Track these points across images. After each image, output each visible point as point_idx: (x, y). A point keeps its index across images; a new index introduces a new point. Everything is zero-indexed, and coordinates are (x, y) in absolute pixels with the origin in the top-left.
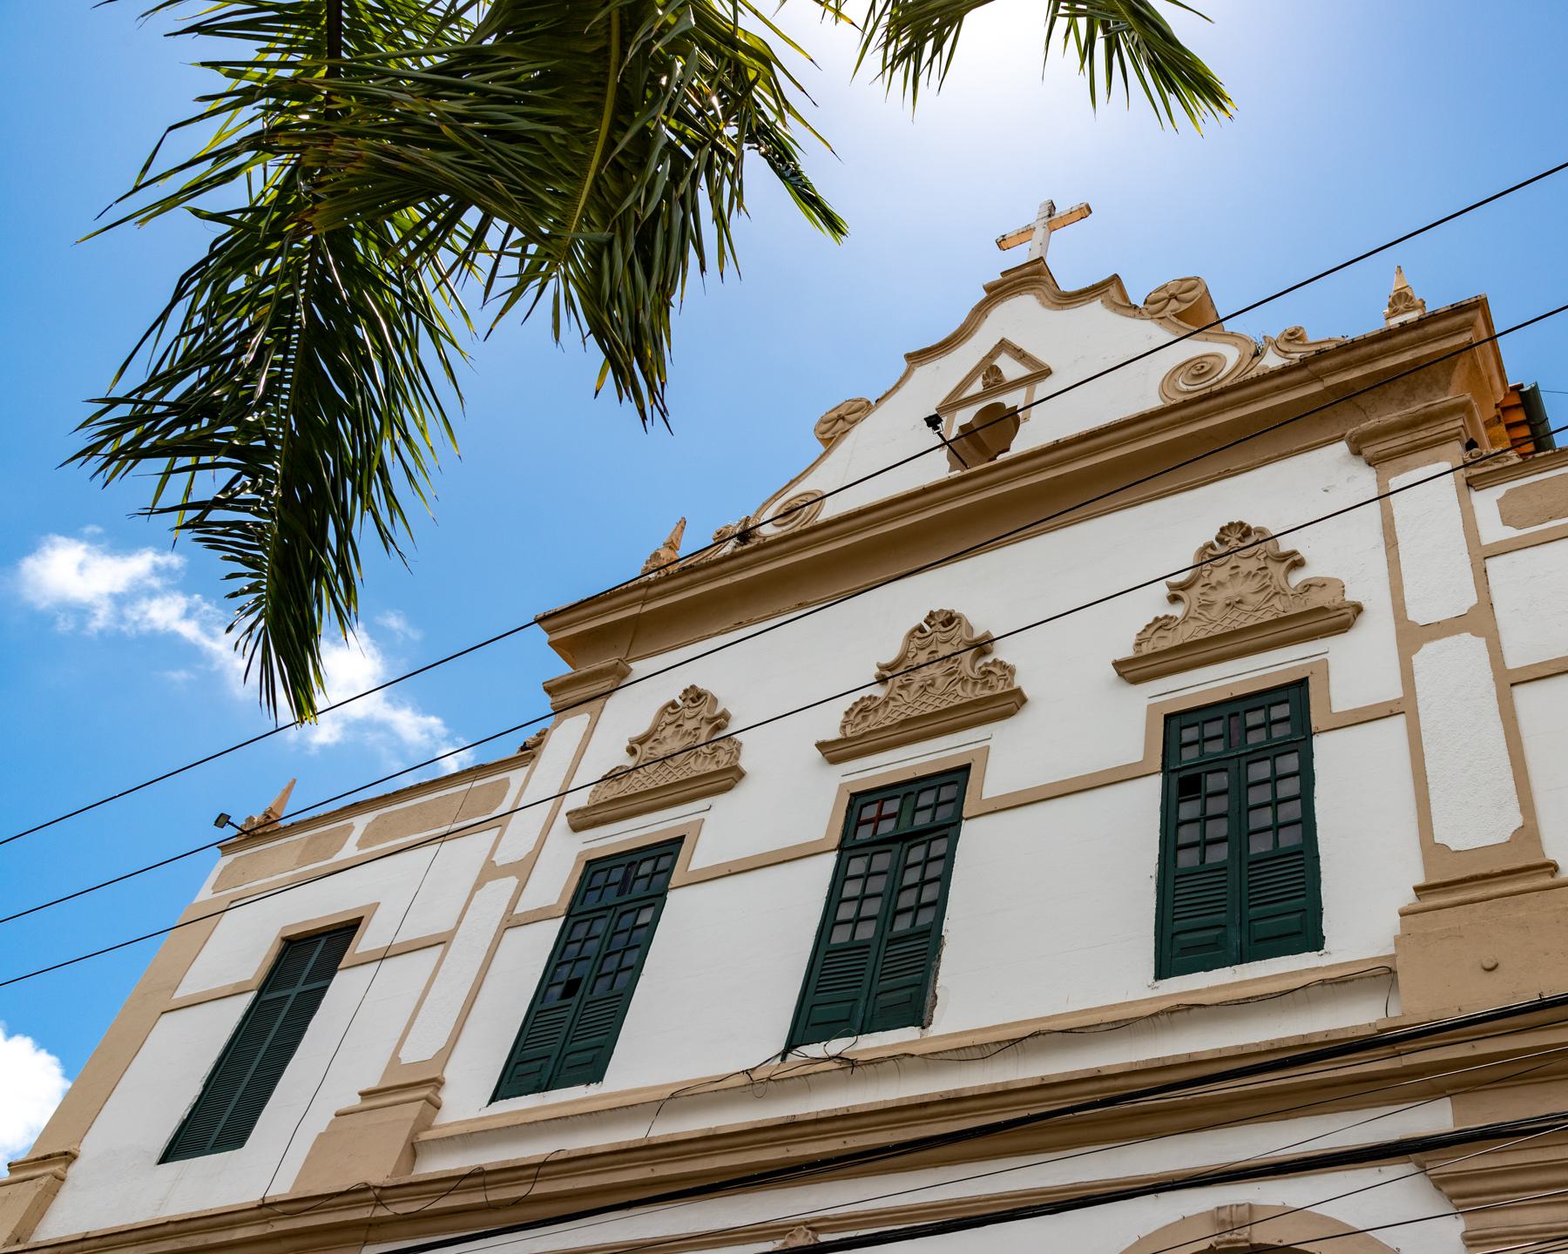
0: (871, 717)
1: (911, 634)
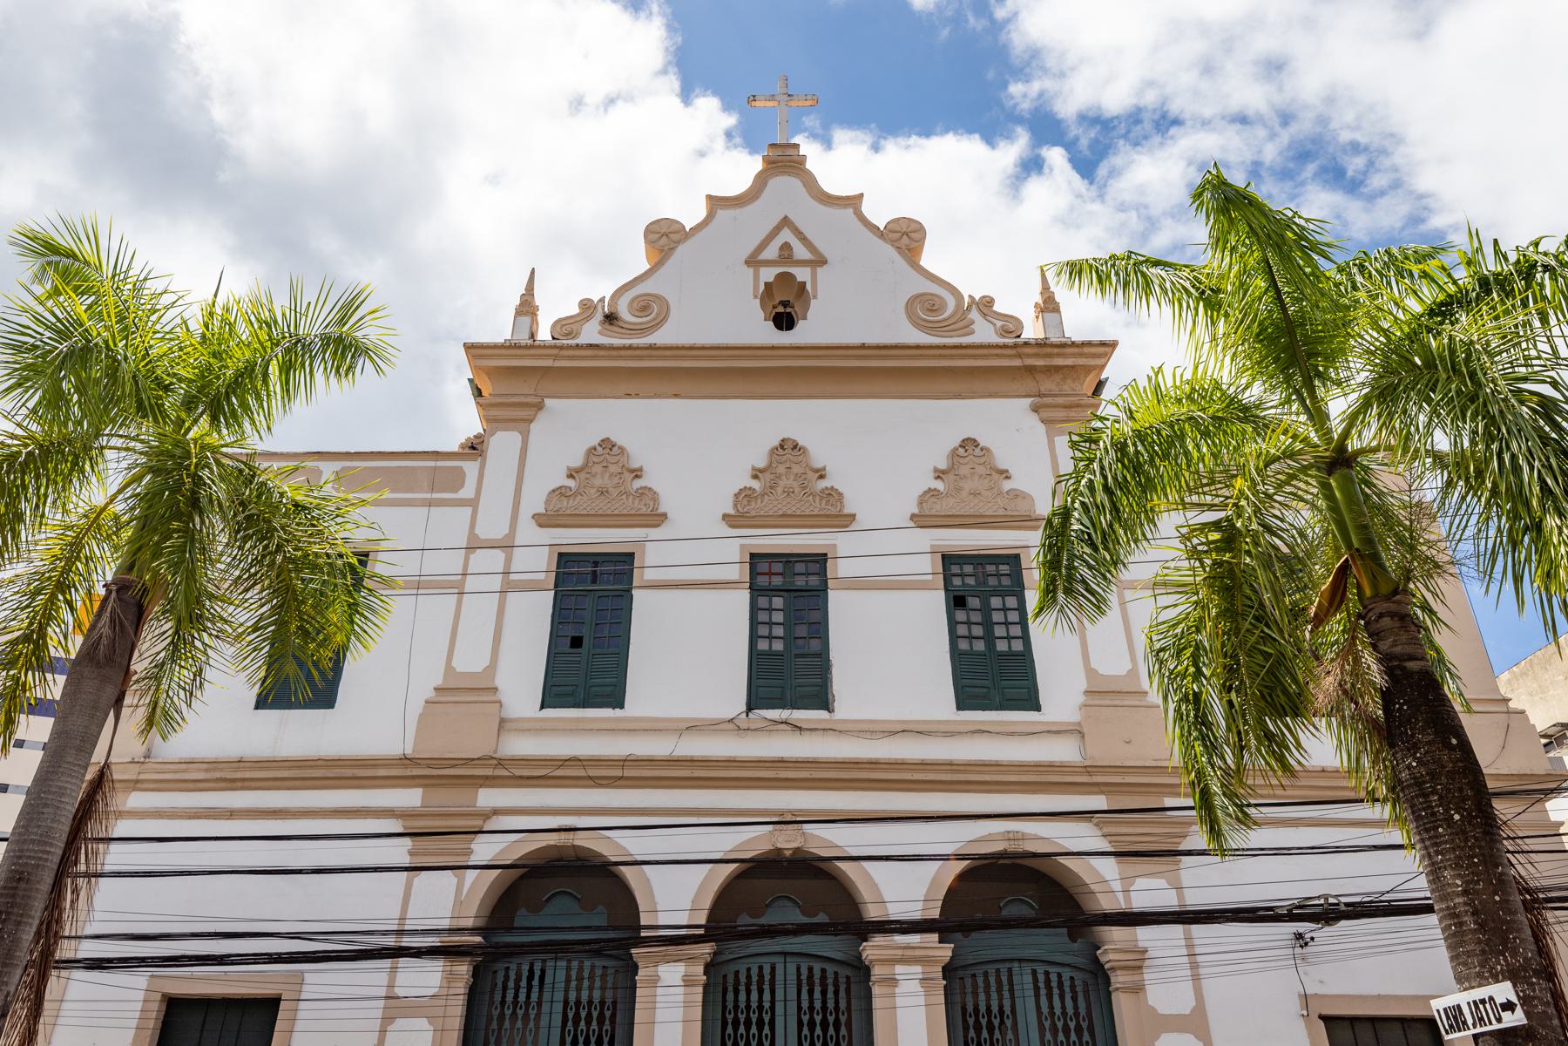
0: (753, 503)
1: (773, 451)
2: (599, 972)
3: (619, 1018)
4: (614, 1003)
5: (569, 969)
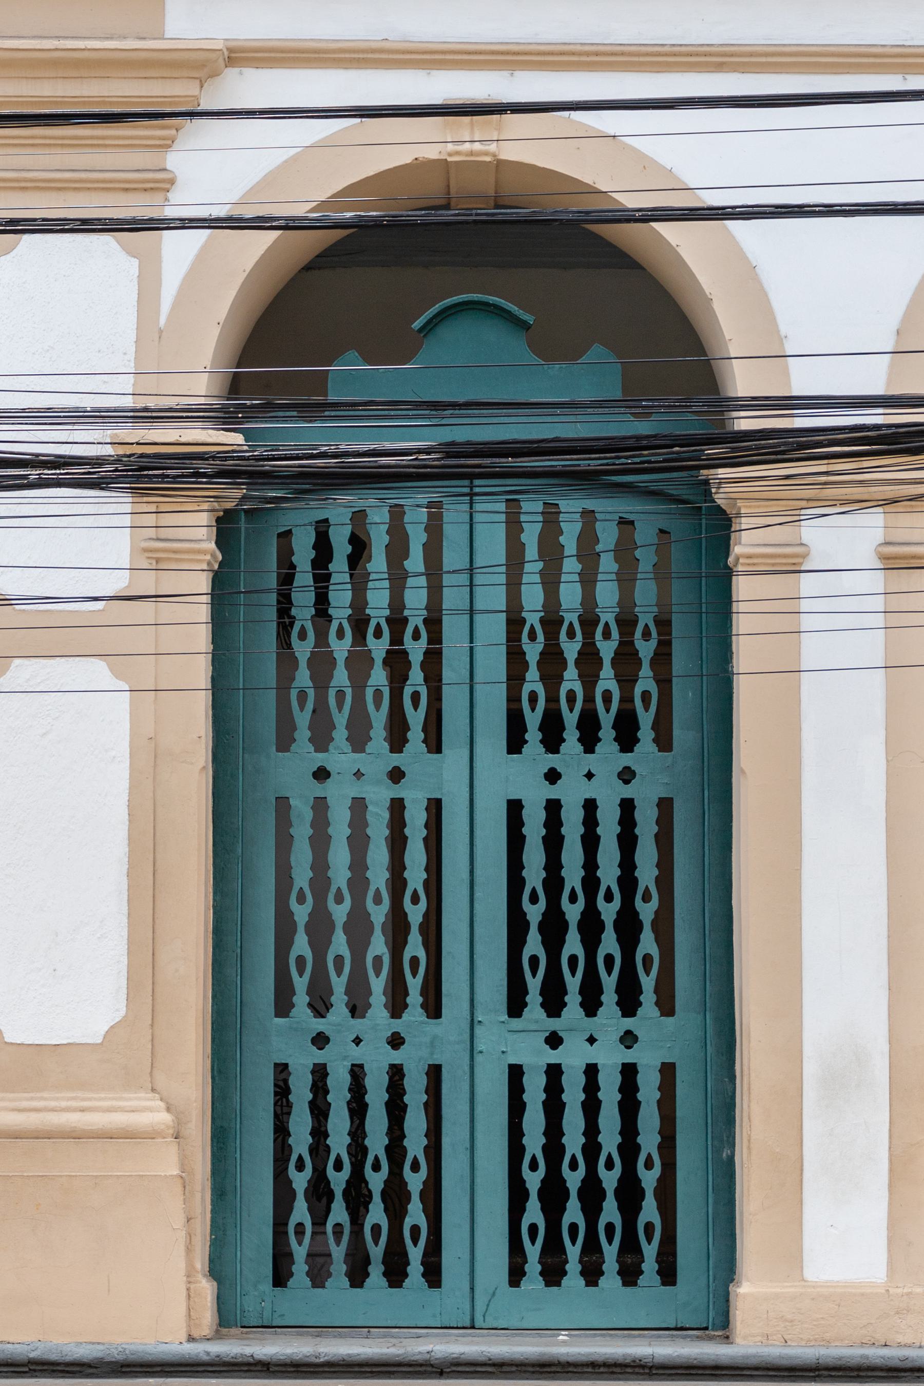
2: (607, 535)
3: (680, 662)
4: (664, 623)
5: (514, 526)
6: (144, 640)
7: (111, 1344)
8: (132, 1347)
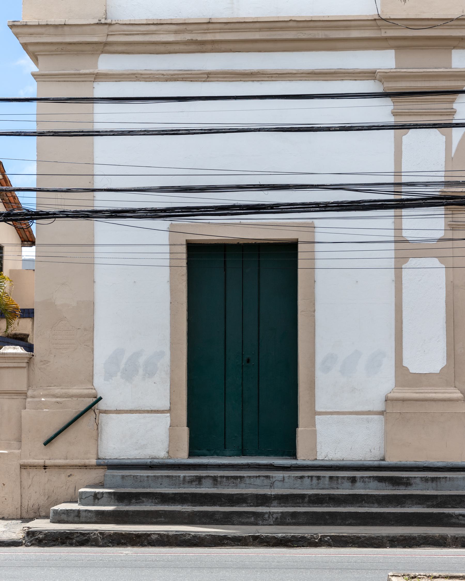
6: (449, 252)
7: (448, 462)
8: (454, 463)
